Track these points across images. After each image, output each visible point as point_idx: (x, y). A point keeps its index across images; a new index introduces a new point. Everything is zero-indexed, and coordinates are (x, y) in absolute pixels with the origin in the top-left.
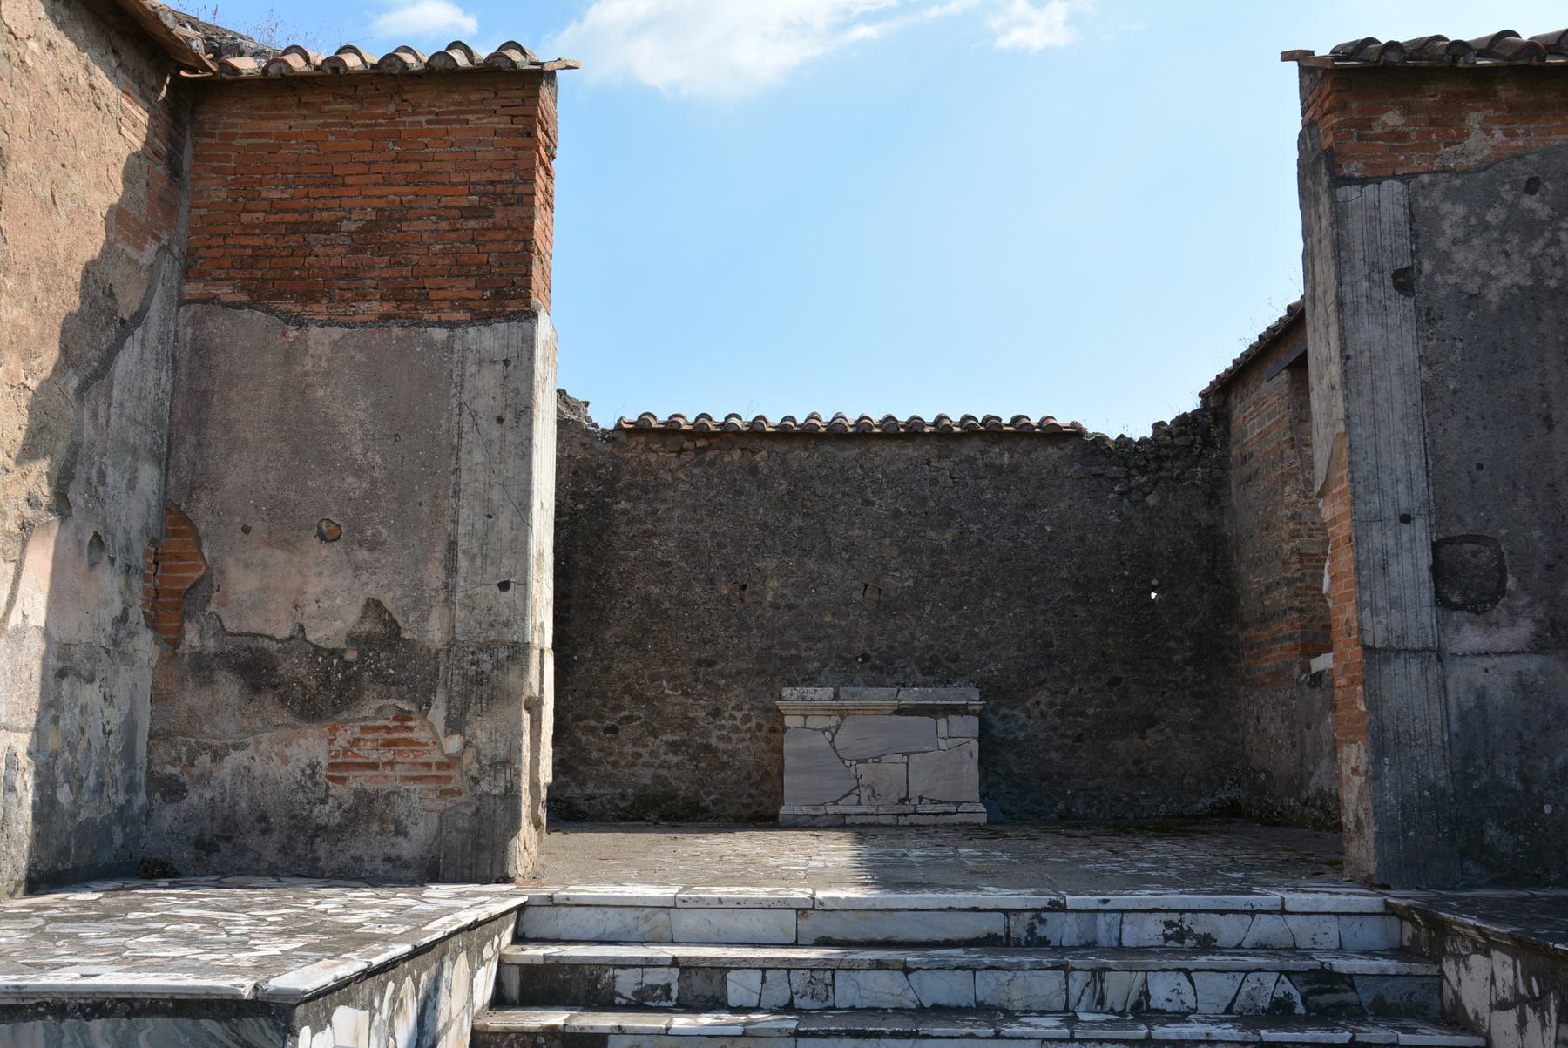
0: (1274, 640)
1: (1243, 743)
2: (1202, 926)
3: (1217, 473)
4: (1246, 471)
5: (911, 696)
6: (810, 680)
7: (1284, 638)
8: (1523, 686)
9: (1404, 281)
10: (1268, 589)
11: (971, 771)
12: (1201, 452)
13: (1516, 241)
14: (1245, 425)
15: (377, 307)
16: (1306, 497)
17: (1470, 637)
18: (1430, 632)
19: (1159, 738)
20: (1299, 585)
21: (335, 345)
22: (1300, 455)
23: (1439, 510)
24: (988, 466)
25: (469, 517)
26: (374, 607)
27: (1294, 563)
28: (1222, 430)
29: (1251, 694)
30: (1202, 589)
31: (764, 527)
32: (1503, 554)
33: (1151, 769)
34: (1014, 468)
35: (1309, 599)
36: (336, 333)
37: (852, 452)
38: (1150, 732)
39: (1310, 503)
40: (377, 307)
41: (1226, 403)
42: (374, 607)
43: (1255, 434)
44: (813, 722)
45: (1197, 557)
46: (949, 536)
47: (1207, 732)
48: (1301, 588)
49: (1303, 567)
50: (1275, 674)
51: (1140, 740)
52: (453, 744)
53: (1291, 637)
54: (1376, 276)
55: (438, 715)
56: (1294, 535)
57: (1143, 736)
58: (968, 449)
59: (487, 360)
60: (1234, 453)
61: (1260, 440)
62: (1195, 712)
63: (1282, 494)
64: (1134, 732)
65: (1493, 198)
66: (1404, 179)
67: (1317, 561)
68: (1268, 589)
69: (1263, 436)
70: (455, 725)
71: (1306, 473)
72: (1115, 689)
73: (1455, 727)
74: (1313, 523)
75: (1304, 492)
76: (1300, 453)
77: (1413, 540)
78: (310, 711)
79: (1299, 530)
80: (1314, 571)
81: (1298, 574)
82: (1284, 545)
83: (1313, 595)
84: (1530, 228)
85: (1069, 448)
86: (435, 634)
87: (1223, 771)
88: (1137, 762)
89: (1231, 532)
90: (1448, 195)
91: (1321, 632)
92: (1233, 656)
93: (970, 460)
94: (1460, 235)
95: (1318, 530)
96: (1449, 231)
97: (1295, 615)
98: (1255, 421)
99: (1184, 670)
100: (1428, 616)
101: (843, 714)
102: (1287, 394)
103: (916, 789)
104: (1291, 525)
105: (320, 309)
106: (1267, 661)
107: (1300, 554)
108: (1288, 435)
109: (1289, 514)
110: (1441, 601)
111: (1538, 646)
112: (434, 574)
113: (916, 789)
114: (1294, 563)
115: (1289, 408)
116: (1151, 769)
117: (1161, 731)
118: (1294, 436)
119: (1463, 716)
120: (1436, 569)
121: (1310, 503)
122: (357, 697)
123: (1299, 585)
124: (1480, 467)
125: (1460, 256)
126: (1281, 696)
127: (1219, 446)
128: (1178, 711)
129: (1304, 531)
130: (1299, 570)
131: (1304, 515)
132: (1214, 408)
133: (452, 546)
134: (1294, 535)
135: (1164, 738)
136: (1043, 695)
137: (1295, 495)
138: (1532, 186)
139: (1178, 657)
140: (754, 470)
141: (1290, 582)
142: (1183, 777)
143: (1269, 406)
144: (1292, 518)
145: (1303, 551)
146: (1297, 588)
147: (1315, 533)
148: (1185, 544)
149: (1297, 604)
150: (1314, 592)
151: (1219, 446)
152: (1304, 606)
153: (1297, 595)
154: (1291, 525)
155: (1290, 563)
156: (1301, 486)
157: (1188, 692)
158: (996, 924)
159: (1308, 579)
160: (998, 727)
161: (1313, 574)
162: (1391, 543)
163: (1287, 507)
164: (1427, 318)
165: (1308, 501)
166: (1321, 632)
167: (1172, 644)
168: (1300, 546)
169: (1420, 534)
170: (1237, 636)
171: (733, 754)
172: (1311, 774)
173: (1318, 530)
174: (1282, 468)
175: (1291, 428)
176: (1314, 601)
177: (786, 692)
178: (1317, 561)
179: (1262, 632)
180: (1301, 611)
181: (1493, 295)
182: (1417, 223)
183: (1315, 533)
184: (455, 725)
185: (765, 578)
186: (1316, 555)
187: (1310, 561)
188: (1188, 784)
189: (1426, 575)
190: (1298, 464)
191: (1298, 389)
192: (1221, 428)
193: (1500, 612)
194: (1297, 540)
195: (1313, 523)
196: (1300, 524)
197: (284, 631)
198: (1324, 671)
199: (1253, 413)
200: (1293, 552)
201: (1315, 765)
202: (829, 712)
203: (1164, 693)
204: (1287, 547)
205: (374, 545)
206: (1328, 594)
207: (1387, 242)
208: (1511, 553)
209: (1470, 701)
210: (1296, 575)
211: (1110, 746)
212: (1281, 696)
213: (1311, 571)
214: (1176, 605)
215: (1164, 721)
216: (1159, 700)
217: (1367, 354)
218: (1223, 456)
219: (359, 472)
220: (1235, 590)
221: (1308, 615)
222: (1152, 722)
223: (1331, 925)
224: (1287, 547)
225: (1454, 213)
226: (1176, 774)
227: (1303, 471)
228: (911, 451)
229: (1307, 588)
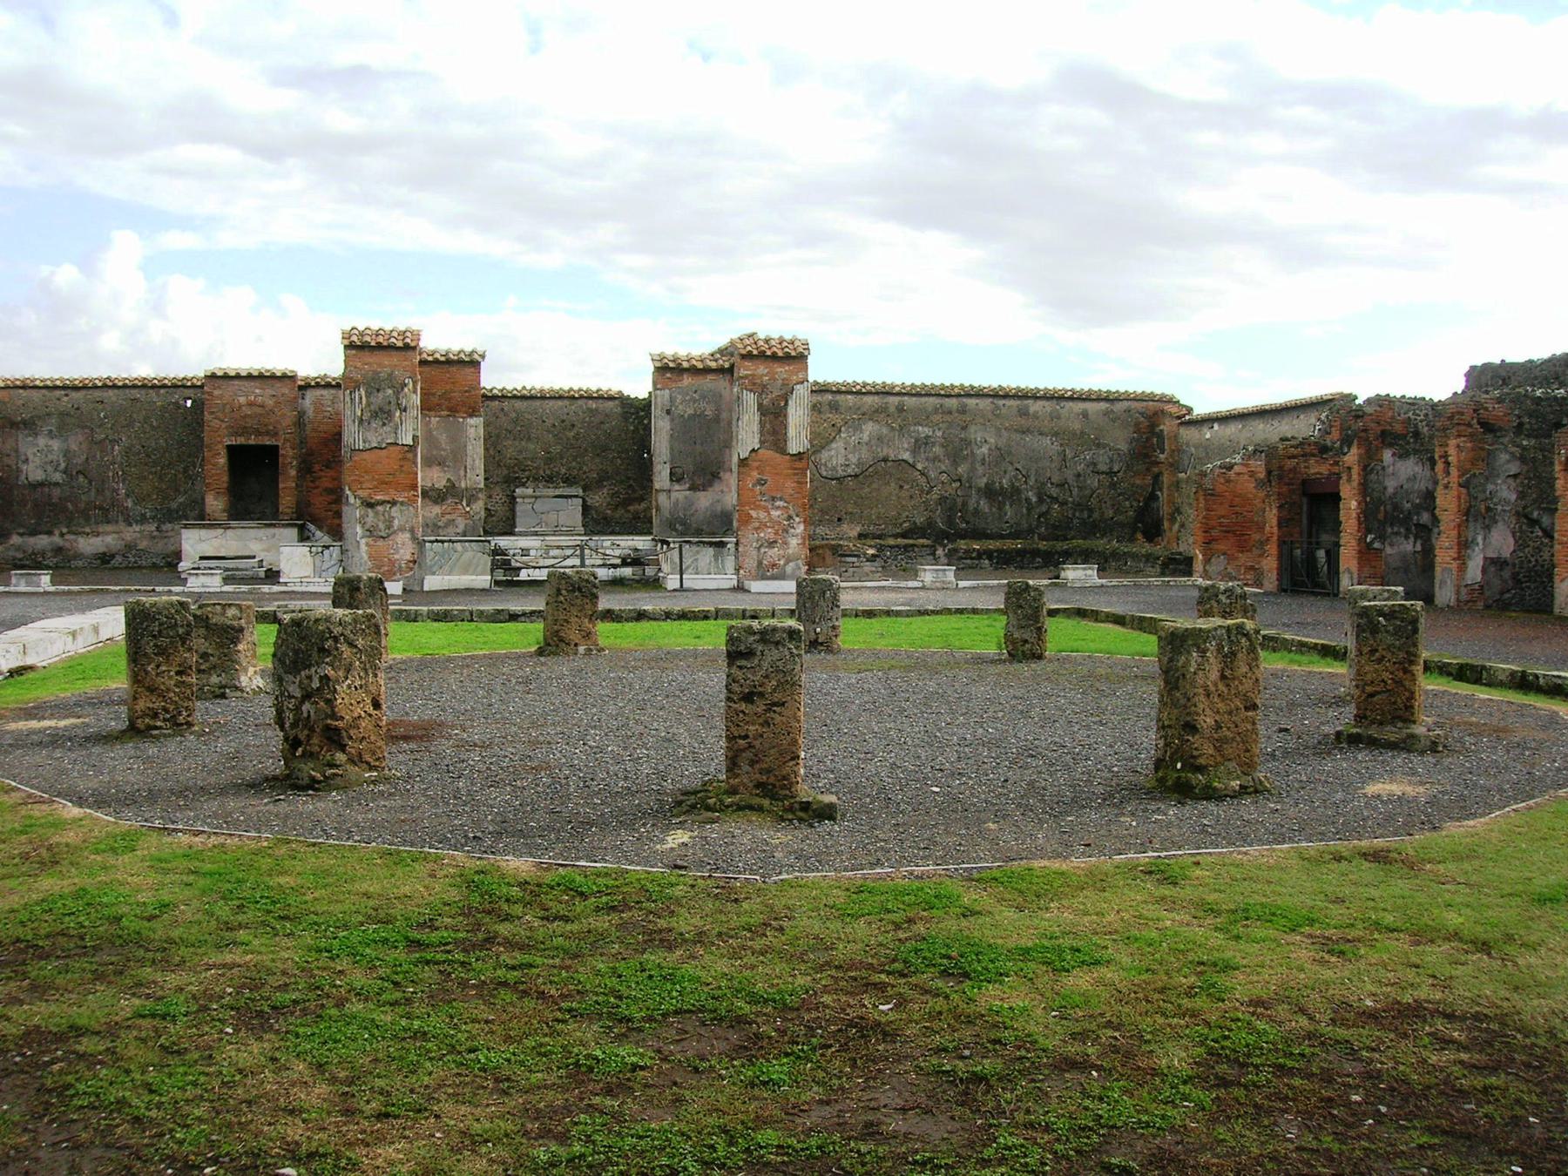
2: (618, 543)
5: (558, 492)
6: (523, 485)
8: (686, 498)
9: (668, 412)
11: (579, 517)
15: (446, 413)
17: (677, 487)
21: (438, 422)
23: (672, 461)
24: (588, 409)
25: (469, 460)
26: (449, 480)
31: (506, 430)
34: (596, 410)
36: (437, 419)
37: (538, 403)
40: (446, 413)
42: (449, 480)
44: (526, 500)
46: (572, 434)
52: (468, 509)
55: (464, 503)
58: (580, 402)
59: (472, 426)
65: (688, 394)
66: (670, 389)
70: (467, 505)
78: (436, 502)
84: (695, 401)
85: (617, 402)
86: (463, 485)
90: (679, 393)
93: (581, 406)
100: (668, 482)
101: (536, 498)
103: (561, 523)
105: (432, 413)
110: (671, 480)
111: (690, 489)
112: (462, 473)
113: (561, 523)
120: (671, 473)
122: (447, 499)
125: (680, 407)
133: (466, 467)
136: (605, 491)
138: (696, 392)
140: (502, 410)
158: (579, 543)
160: (589, 502)
164: (672, 420)
169: (668, 466)
171: (496, 511)
177: (517, 490)
181: (686, 416)
182: (672, 399)
184: (467, 505)
185: (507, 449)
193: (682, 482)
197: (430, 485)
202: (532, 497)
205: (448, 467)
219: (444, 450)
223: (642, 543)
225: (680, 397)
228: (560, 403)
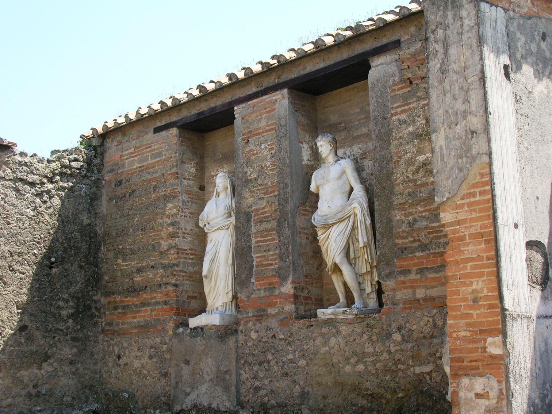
0: (143, 304)
1: (100, 372)
3: (94, 189)
4: (120, 191)
7: (158, 303)
10: (139, 271)
12: (85, 175)
13: (541, 66)
14: (124, 160)
16: (182, 212)
18: (527, 301)
19: (50, 369)
20: (176, 269)
22: (181, 185)
27: (174, 254)
28: (99, 162)
29: (113, 340)
30: (81, 267)
32: (547, 254)
33: (44, 391)
35: (181, 278)
38: (45, 366)
39: (185, 216)
41: (102, 144)
43: (135, 167)
45: (79, 245)
47: (80, 365)
48: (177, 271)
49: (179, 257)
50: (144, 328)
51: (37, 371)
53: (165, 303)
54: (497, 64)
56: (173, 236)
57: (40, 369)
60: (106, 178)
61: (139, 171)
62: (73, 351)
63: (164, 208)
64: (35, 365)
67: (187, 254)
68: (139, 271)
69: (142, 169)
71: (183, 196)
72: (24, 333)
73: (539, 364)
74: (186, 229)
75: (182, 209)
76: (181, 182)
77: (519, 240)
79: (178, 233)
80: (184, 260)
81: (175, 262)
82: (163, 242)
83: (183, 276)
87: (88, 392)
88: (35, 386)
89: (100, 230)
91: (186, 300)
92: (97, 314)
94: (524, 53)
95: (188, 234)
96: (520, 49)
97: (170, 288)
98: (136, 158)
99: (68, 322)
102: (176, 144)
104: (171, 229)
106: (135, 317)
107: (178, 249)
108: (174, 170)
109: (169, 222)
114: (174, 254)
115: (176, 153)
116: (44, 391)
117: (52, 364)
118: (178, 171)
119: (541, 358)
121: (185, 216)
123: (176, 269)
124: (538, 198)
126: (149, 342)
127: (96, 172)
128: (62, 350)
129: (181, 235)
130: (176, 259)
131: (181, 223)
132: (95, 146)
134: (173, 236)
135: (53, 369)
137: (175, 210)
139: (64, 313)
141: (165, 267)
142: (64, 396)
143: (154, 150)
144: (173, 224)
145: (179, 247)
146: (175, 270)
147: (186, 236)
148: (73, 235)
149: (173, 281)
150: (185, 274)
151: (96, 172)
152: (178, 282)
153: (175, 275)
154: (171, 229)
155: (167, 254)
156: (181, 204)
157: (69, 337)
159: (181, 265)
161: (184, 262)
162: (512, 241)
163: (168, 217)
165: (183, 214)
166: (186, 300)
167: (61, 303)
168: (178, 243)
170: (100, 300)
172: (188, 394)
173: (188, 234)
174: (165, 191)
175: (177, 166)
176: (184, 280)
178: (187, 254)
179: (129, 299)
180: (176, 285)
183: (186, 236)
186: (186, 250)
187: (182, 253)
188: (67, 401)
189: (524, 263)
190: (179, 190)
191: (182, 141)
192: (98, 161)
194: (177, 239)
195: (186, 229)
196: (179, 229)
198: (206, 326)
199: (131, 153)
200: (170, 247)
201: (193, 388)
203: (54, 337)
204: (164, 245)
206: (206, 277)
207: (500, 46)
208: (550, 255)
209: (543, 349)
210: (172, 262)
211: (18, 375)
212: (149, 342)
213: (182, 260)
214: (65, 276)
215: (54, 357)
216: (51, 342)
217: (497, 114)
218: (98, 179)
220: (100, 269)
221: (180, 289)
222: (47, 357)
224: (164, 245)
226: (60, 394)
227: (182, 195)
229: (180, 271)
